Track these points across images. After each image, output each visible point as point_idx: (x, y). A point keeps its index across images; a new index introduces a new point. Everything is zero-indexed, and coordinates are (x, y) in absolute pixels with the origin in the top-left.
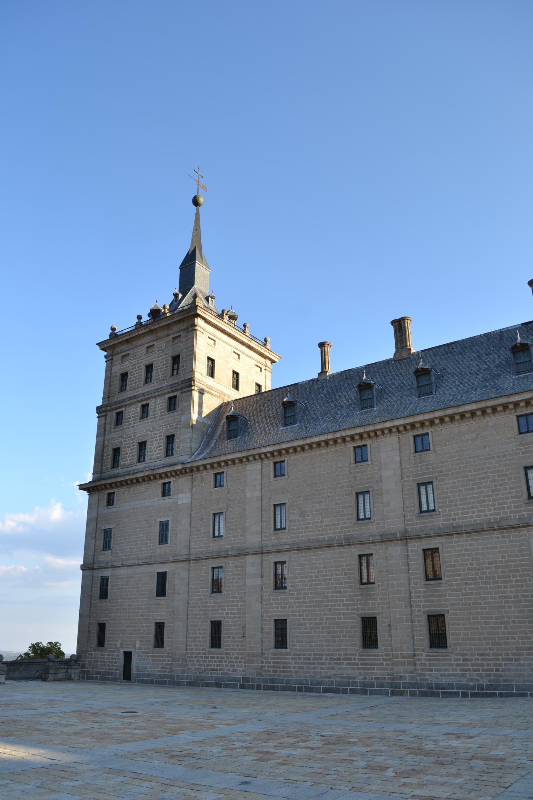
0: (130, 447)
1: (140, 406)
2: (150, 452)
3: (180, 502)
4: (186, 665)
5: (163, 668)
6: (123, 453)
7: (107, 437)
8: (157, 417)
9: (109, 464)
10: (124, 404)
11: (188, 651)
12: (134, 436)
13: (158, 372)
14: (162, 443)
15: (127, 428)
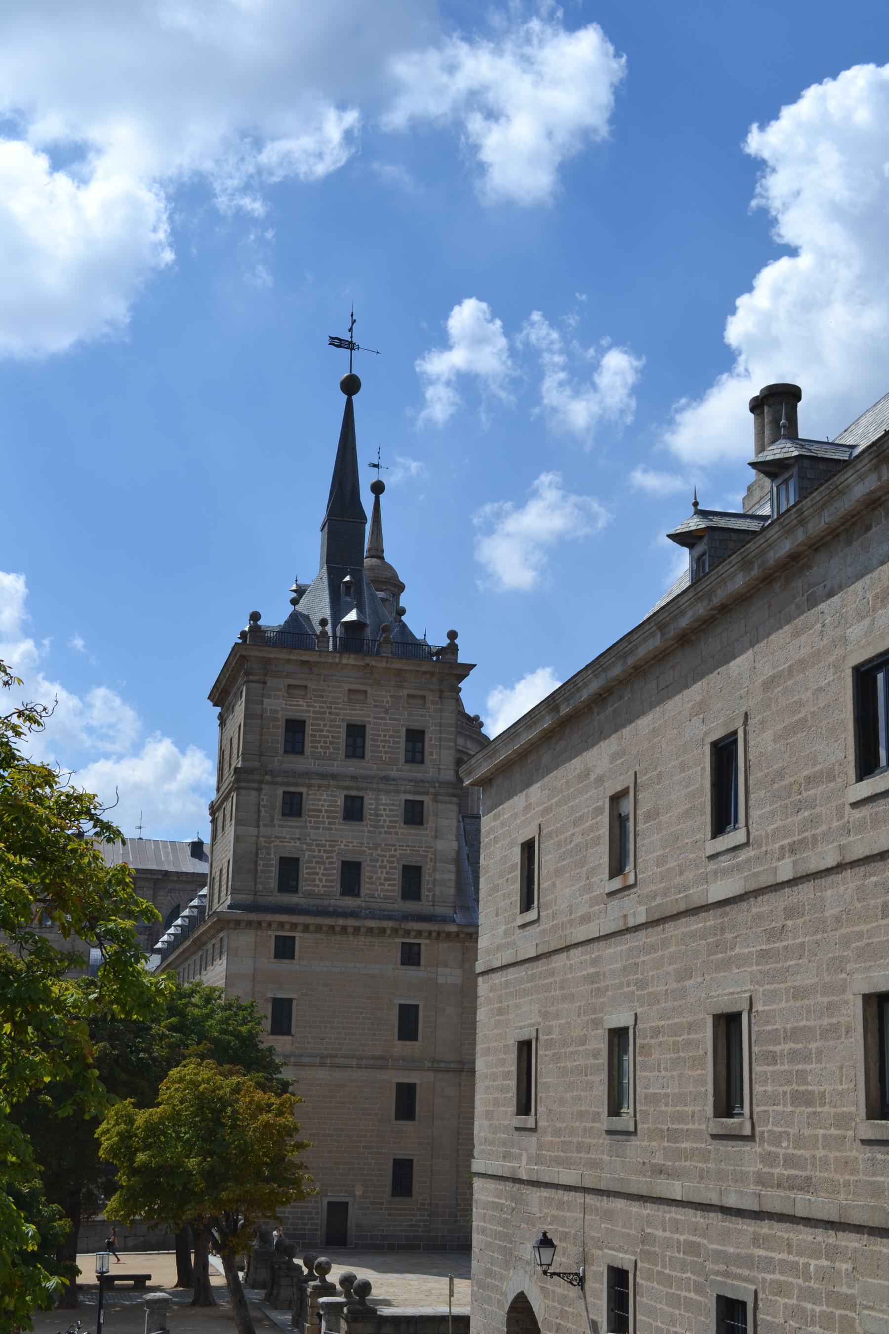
0: (323, 863)
1: (343, 796)
2: (372, 884)
3: (441, 980)
4: (456, 1221)
5: (411, 1226)
6: (305, 871)
7: (263, 830)
8: (383, 827)
9: (273, 883)
10: (307, 781)
11: (459, 1202)
12: (334, 846)
13: (378, 746)
14: (395, 874)
15: (312, 828)
